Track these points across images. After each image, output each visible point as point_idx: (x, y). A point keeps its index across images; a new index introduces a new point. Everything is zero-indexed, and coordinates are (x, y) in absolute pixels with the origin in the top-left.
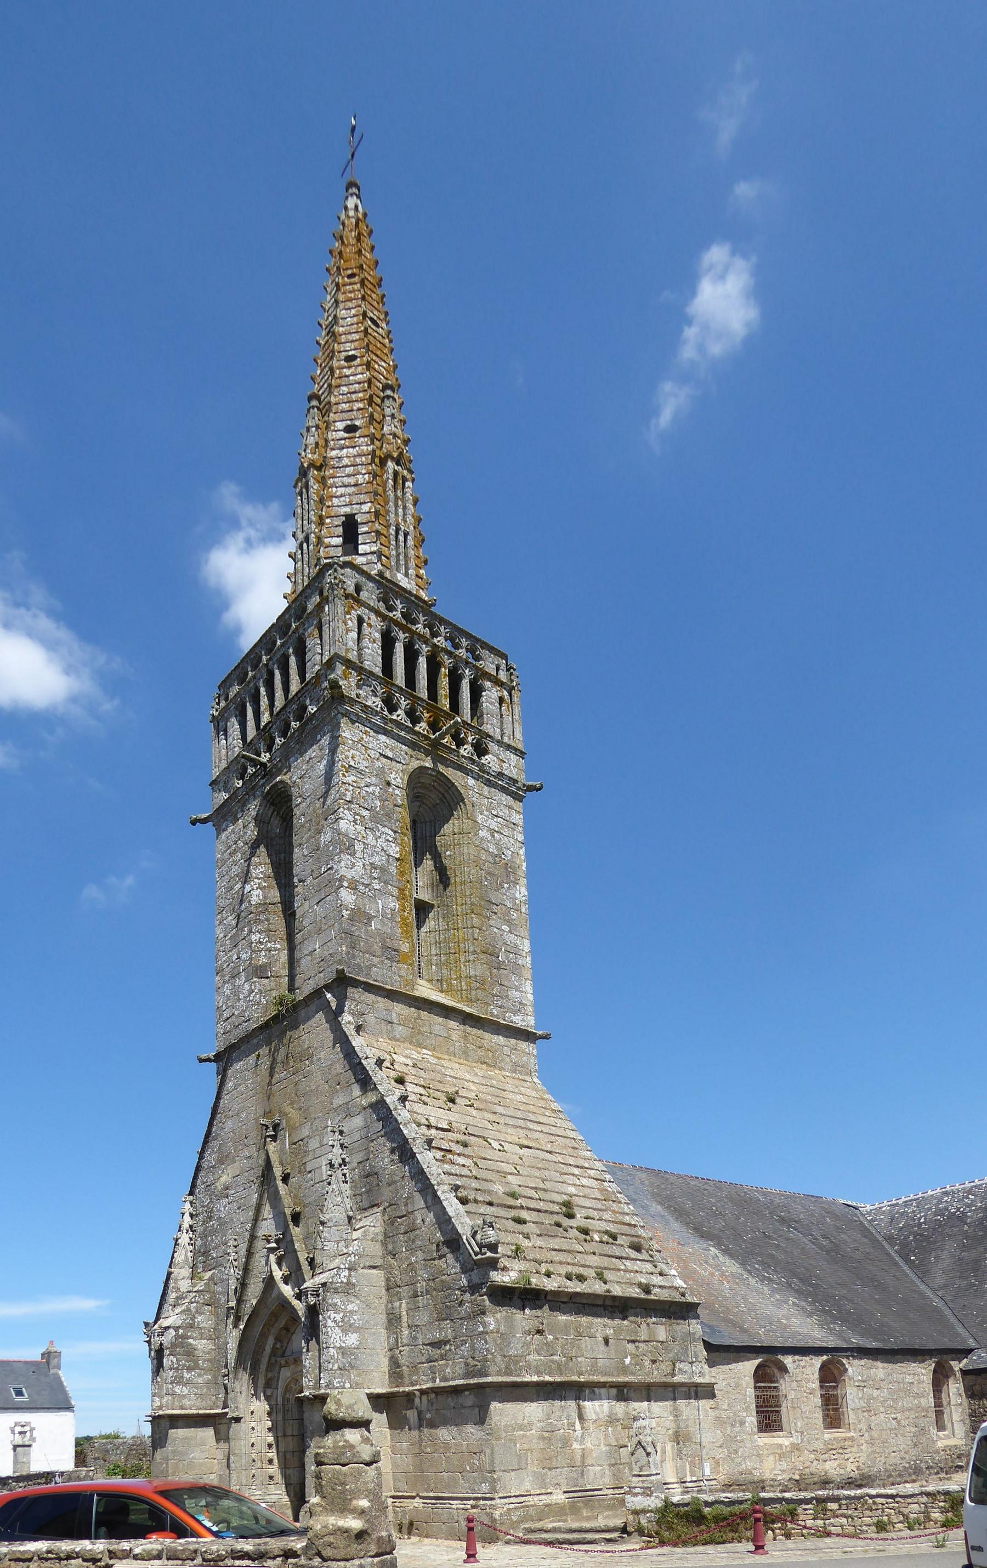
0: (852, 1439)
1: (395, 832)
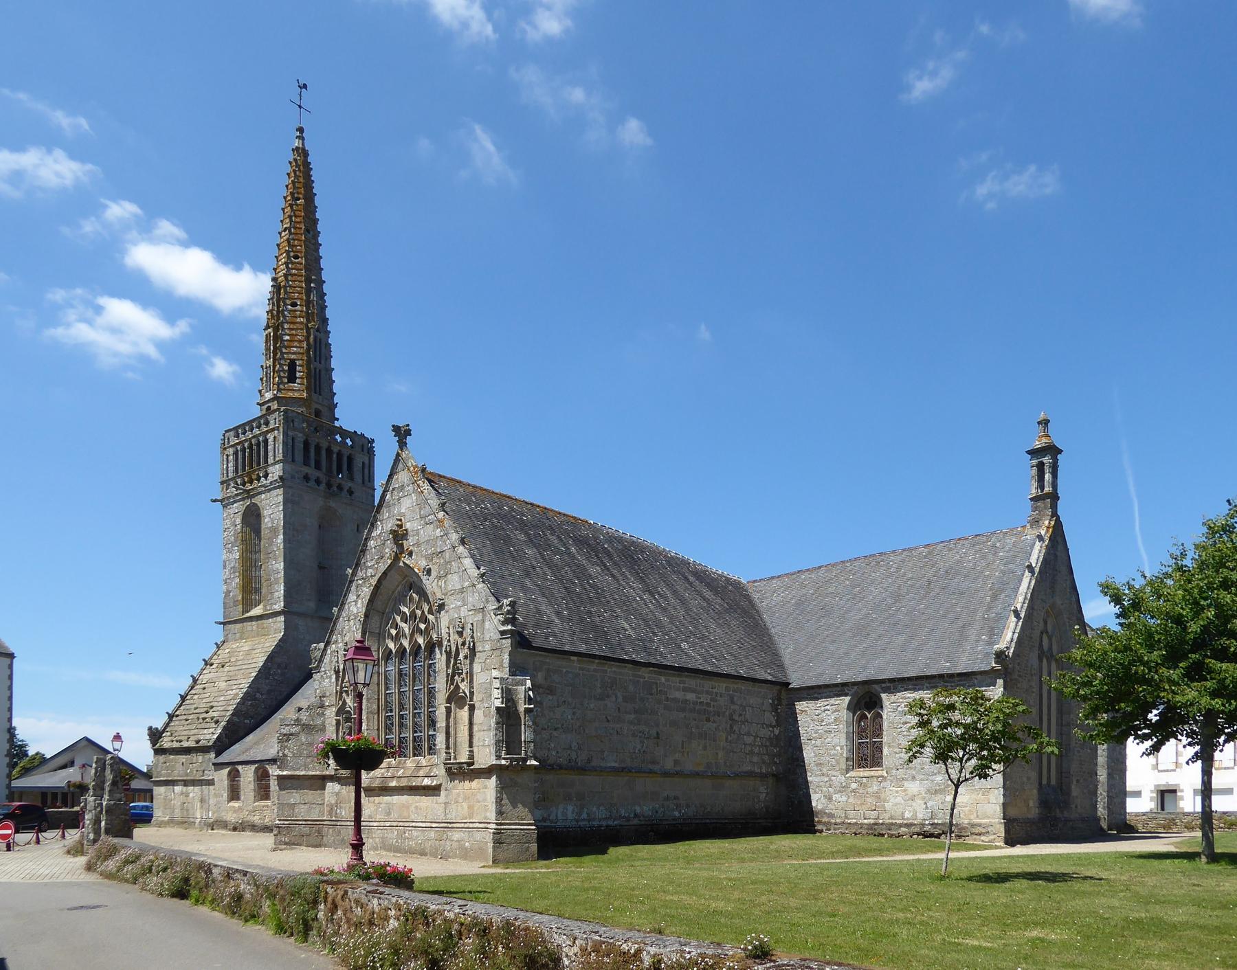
0: (267, 806)
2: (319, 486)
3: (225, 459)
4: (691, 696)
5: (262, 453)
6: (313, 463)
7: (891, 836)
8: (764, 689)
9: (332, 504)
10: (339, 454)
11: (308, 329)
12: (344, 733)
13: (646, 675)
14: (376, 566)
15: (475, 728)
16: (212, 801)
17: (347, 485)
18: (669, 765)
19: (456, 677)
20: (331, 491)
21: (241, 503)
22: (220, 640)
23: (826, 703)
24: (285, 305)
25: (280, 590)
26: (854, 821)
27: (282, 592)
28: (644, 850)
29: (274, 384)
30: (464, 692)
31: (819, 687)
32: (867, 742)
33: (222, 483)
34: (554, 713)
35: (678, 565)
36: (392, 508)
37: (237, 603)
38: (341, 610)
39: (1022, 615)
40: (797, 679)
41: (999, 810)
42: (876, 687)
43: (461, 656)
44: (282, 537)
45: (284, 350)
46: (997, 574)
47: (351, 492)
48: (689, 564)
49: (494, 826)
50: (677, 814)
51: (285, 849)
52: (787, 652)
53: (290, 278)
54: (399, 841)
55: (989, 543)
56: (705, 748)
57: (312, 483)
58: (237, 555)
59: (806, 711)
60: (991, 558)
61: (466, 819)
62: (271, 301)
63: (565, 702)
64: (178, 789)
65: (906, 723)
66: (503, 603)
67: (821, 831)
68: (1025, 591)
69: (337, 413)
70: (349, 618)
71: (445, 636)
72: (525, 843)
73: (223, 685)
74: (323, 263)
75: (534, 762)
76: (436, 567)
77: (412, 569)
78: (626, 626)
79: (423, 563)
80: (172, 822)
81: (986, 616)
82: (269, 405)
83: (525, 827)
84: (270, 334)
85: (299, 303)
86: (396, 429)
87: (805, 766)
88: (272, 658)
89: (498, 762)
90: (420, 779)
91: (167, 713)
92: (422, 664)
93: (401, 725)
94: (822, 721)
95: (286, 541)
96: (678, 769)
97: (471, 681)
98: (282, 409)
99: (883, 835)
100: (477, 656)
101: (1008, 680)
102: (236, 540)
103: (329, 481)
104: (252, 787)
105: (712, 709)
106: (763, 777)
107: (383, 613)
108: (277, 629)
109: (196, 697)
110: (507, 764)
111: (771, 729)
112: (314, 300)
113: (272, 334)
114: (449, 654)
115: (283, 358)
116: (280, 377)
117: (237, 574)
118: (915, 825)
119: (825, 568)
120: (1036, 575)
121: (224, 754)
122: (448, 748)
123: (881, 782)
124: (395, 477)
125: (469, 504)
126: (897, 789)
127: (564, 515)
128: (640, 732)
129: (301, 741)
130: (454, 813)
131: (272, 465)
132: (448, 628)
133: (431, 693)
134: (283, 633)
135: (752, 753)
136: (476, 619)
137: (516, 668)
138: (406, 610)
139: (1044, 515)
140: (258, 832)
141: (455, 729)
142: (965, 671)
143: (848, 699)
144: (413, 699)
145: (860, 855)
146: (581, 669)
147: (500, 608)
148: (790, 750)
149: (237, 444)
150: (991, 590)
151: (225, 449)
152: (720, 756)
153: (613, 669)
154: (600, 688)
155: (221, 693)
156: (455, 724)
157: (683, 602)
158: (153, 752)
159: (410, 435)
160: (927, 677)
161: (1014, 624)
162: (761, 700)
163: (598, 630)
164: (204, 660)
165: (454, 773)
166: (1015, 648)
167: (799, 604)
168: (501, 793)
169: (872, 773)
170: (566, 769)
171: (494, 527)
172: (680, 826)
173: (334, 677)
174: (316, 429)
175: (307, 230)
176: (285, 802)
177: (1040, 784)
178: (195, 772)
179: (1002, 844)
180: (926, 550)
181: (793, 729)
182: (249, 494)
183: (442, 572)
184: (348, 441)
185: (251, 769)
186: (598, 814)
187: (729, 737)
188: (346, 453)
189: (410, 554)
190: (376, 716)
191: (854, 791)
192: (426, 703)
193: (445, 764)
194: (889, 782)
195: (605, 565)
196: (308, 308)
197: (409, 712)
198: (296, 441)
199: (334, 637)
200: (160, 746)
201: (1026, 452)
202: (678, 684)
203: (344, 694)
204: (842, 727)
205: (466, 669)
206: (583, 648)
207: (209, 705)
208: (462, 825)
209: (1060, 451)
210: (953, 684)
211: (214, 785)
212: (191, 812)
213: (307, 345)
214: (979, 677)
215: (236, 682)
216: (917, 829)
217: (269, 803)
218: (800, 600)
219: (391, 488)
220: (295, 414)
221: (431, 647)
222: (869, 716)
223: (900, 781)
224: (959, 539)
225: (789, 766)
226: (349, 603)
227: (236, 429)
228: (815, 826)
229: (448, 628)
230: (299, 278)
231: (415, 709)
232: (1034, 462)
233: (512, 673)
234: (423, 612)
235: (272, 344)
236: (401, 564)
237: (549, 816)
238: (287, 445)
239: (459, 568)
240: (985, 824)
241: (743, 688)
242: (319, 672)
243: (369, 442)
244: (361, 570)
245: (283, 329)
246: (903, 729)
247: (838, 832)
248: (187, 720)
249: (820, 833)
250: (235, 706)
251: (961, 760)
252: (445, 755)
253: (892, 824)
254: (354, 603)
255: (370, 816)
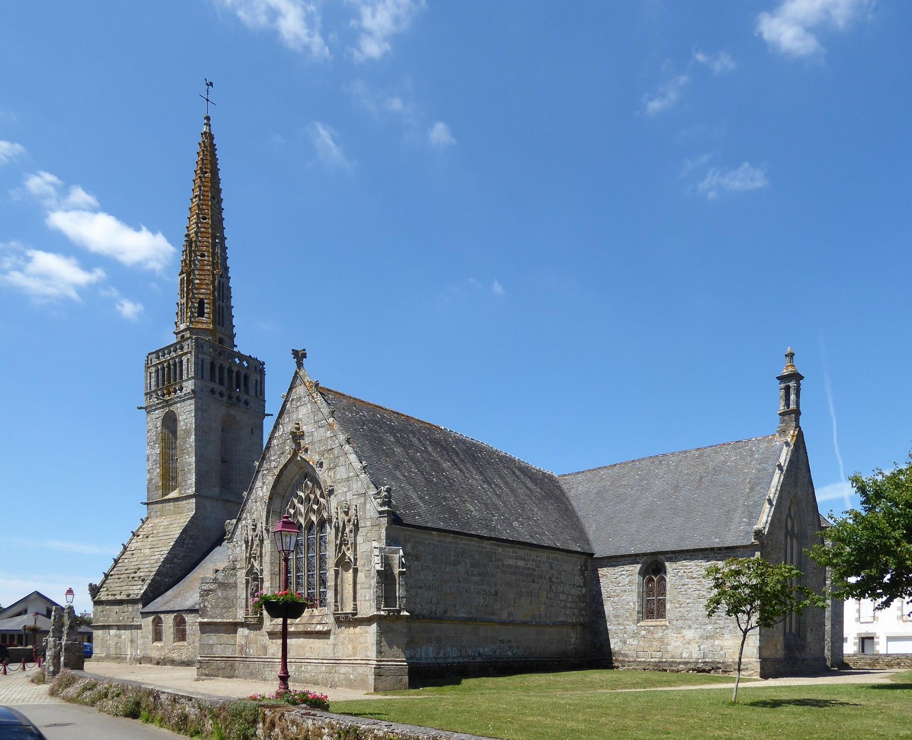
0: (184, 646)
1: (158, 444)
2: (222, 397)
3: (148, 376)
4: (521, 563)
5: (178, 371)
6: (217, 381)
7: (672, 671)
8: (575, 558)
9: (232, 412)
10: (238, 374)
11: (214, 275)
12: (253, 589)
13: (488, 547)
14: (278, 460)
15: (358, 586)
16: (140, 642)
17: (244, 397)
18: (504, 616)
19: (343, 547)
20: (232, 402)
21: (161, 410)
22: (144, 517)
23: (622, 569)
24: (196, 256)
25: (192, 479)
26: (644, 659)
27: (194, 480)
28: (489, 682)
29: (187, 318)
30: (349, 559)
31: (617, 557)
32: (654, 599)
33: (146, 394)
34: (419, 575)
35: (507, 462)
36: (291, 415)
37: (159, 488)
38: (249, 494)
39: (774, 503)
40: (599, 551)
41: (756, 651)
42: (662, 557)
43: (347, 530)
44: (193, 437)
45: (195, 291)
46: (754, 471)
47: (247, 403)
48: (515, 461)
49: (375, 663)
50: (510, 654)
51: (205, 679)
52: (591, 530)
53: (199, 235)
54: (297, 674)
55: (747, 448)
56: (531, 603)
57: (217, 396)
58: (158, 451)
59: (607, 576)
60: (749, 459)
61: (351, 656)
62: (184, 253)
63: (427, 566)
64: (112, 632)
65: (685, 585)
66: (381, 490)
67: (618, 667)
68: (776, 484)
69: (236, 341)
70: (256, 500)
71: (334, 515)
72: (399, 676)
73: (147, 551)
74: (225, 224)
75: (406, 613)
76: (327, 461)
77: (308, 462)
78: (472, 509)
79: (316, 458)
80: (108, 658)
81: (746, 503)
82: (183, 334)
83: (399, 663)
84: (184, 278)
85: (206, 255)
86: (295, 353)
87: (605, 617)
88: (186, 532)
89: (378, 613)
90: (313, 626)
91: (104, 573)
92: (315, 536)
93: (298, 584)
94: (619, 583)
95: (197, 440)
96: (511, 619)
97: (355, 550)
98: (194, 337)
99: (666, 670)
100: (360, 531)
101: (764, 552)
102: (157, 439)
103: (230, 394)
104: (172, 630)
105: (536, 573)
106: (573, 625)
107: (284, 497)
108: (189, 509)
109: (126, 561)
110: (386, 614)
111: (579, 589)
112: (218, 252)
113: (185, 278)
114: (337, 529)
115: (194, 297)
116: (191, 312)
117: (158, 466)
118: (691, 663)
119: (619, 466)
120: (784, 473)
121: (149, 606)
122: (336, 601)
123: (664, 630)
124: (294, 390)
125: (351, 412)
126: (677, 635)
127: (422, 422)
128: (483, 590)
129: (218, 595)
130: (341, 653)
131: (186, 380)
132: (337, 508)
133: (322, 559)
134: (194, 512)
135: (565, 607)
136: (359, 502)
137: (391, 540)
138: (302, 494)
139: (789, 427)
140: (176, 666)
141: (342, 587)
142: (731, 545)
143: (639, 566)
144: (308, 564)
145: (654, 685)
146: (440, 541)
147: (379, 493)
148: (594, 605)
149: (158, 364)
150: (749, 483)
151: (148, 368)
152: (542, 609)
153: (464, 542)
154: (454, 556)
155: (147, 558)
156: (342, 583)
157: (513, 491)
158: (92, 603)
159: (306, 358)
160: (701, 550)
161: (768, 509)
162: (572, 566)
163: (451, 511)
164: (132, 532)
165: (341, 622)
166: (769, 528)
167: (599, 493)
168: (381, 637)
169: (658, 623)
170: (428, 619)
171: (371, 430)
172: (512, 663)
173: (244, 545)
174: (219, 353)
175: (213, 198)
176: (205, 643)
177: (785, 632)
178: (126, 619)
179: (758, 677)
180: (698, 452)
181: (596, 589)
182: (168, 404)
183: (331, 465)
184: (245, 363)
185: (171, 617)
186: (452, 654)
187: (549, 595)
188: (243, 372)
189: (306, 450)
190: (278, 577)
191: (643, 637)
192: (318, 567)
193: (334, 614)
194: (670, 630)
195: (454, 461)
196: (213, 259)
197: (304, 573)
198: (204, 362)
199: (244, 514)
200: (99, 598)
201: (776, 378)
202: (511, 554)
203: (252, 559)
204: (635, 587)
205: (351, 540)
206: (441, 525)
207: (136, 567)
208: (348, 662)
209: (802, 378)
210: (721, 555)
211: (141, 629)
212: (123, 650)
213: (213, 287)
214: (741, 550)
215: (158, 550)
216: (692, 666)
217: (185, 643)
218: (600, 490)
219: (290, 399)
220: (204, 342)
221: (322, 523)
222: (655, 579)
223: (679, 630)
224: (724, 445)
225: (593, 618)
226: (256, 488)
227: (157, 352)
228: (613, 663)
229: (337, 508)
230: (207, 235)
231: (309, 571)
232: (783, 386)
233: (388, 544)
234: (316, 496)
235: (185, 286)
236: (299, 458)
237: (415, 655)
238: (198, 366)
239: (346, 462)
240: (745, 662)
241: (559, 557)
242: (232, 542)
243: (261, 364)
244: (266, 463)
245: (194, 275)
246: (682, 590)
247: (631, 668)
248: (119, 579)
249: (617, 668)
250: (157, 568)
251: (748, 613)
252: (334, 607)
253: (673, 662)
254: (260, 489)
255: (273, 654)
